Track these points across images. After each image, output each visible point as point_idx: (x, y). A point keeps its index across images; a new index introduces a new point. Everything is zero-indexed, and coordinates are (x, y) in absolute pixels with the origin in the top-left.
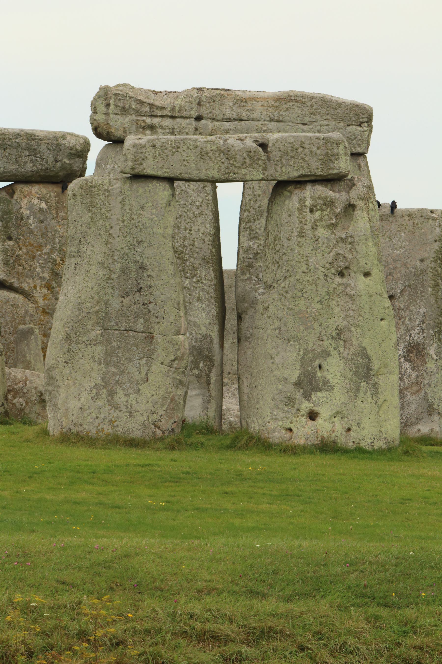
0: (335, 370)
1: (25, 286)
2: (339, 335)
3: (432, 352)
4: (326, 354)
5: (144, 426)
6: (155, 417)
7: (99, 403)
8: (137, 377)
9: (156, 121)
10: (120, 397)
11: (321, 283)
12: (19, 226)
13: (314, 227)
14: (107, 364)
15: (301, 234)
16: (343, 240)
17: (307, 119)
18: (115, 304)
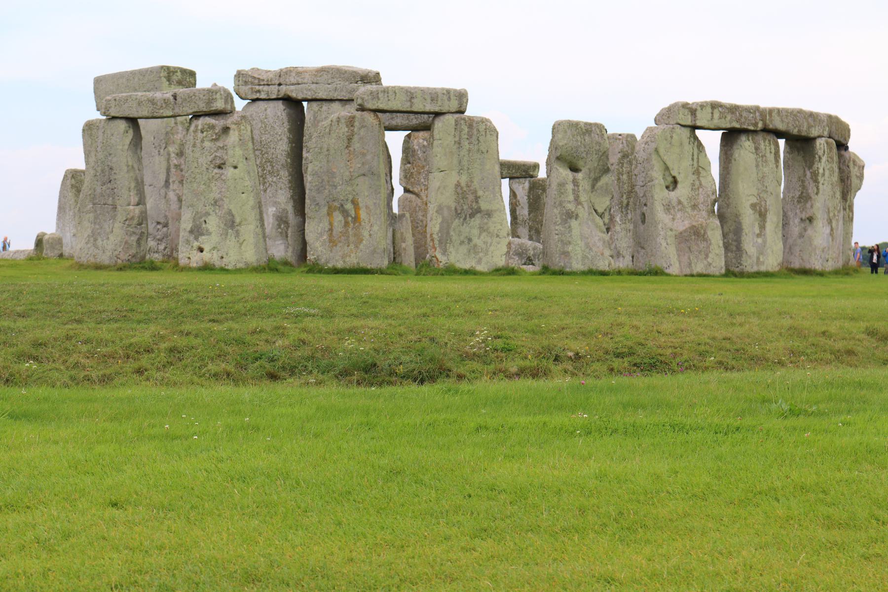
0: (213, 223)
1: (416, 190)
2: (216, 203)
3: (618, 219)
4: (207, 214)
5: (111, 258)
6: (116, 253)
7: (89, 245)
8: (108, 230)
9: (261, 87)
10: (99, 242)
11: (205, 173)
12: (413, 156)
13: (202, 141)
14: (95, 223)
15: (194, 146)
16: (222, 148)
17: (330, 81)
18: (99, 190)
